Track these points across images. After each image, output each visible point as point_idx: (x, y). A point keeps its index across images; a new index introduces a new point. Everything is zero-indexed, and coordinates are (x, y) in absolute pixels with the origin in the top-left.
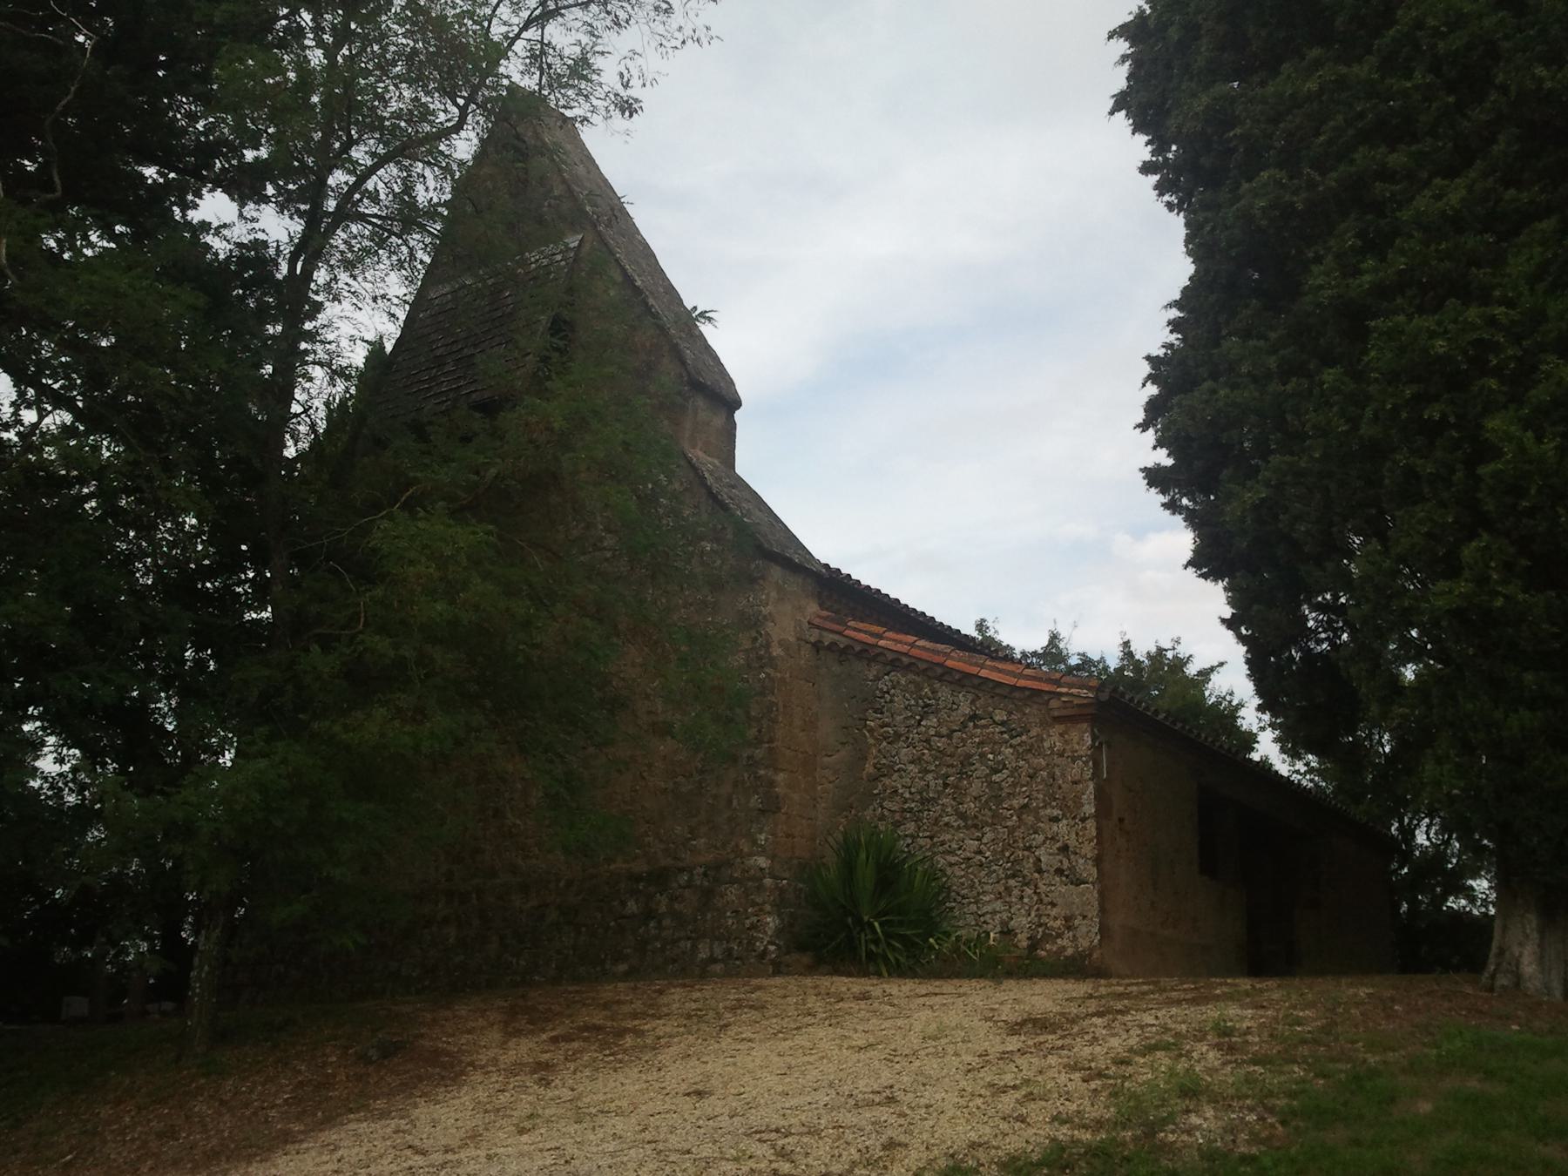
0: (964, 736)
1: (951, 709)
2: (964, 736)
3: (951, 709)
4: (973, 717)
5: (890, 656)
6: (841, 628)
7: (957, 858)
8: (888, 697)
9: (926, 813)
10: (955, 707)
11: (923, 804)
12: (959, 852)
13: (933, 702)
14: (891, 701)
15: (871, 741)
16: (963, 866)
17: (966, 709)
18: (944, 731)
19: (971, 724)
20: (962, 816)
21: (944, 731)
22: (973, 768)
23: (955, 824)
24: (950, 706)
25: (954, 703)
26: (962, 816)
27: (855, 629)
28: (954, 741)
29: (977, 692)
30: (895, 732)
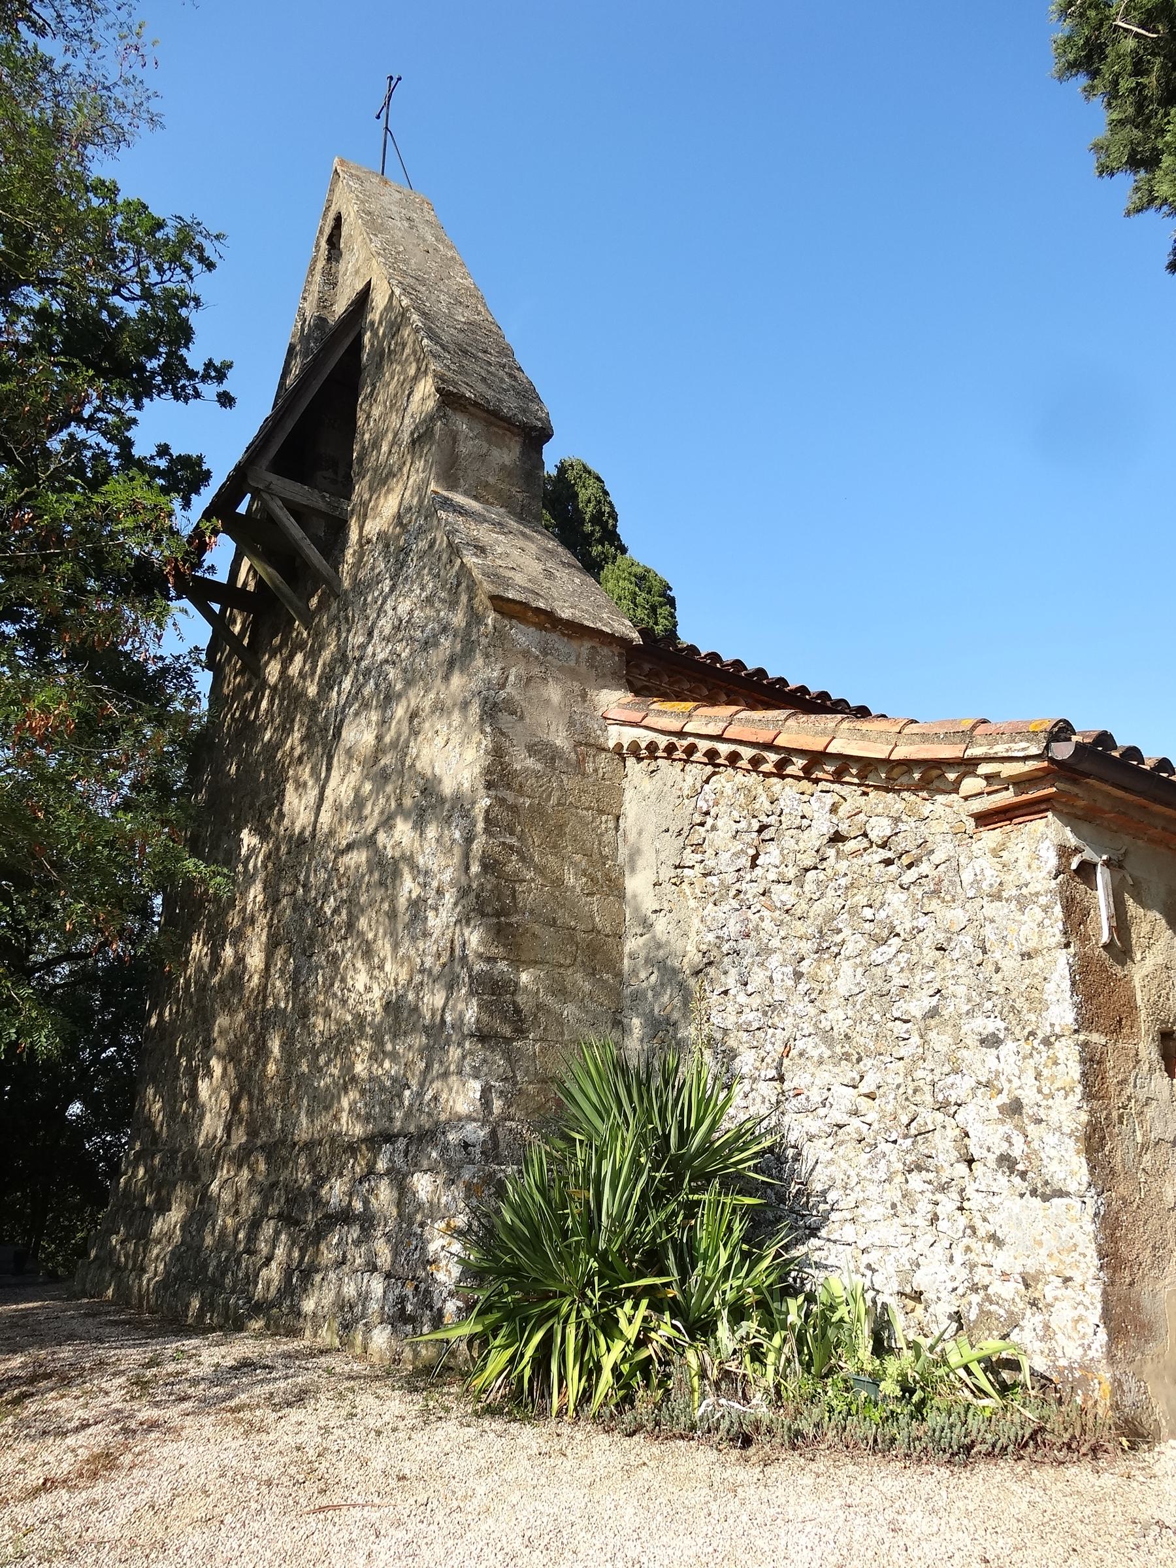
0: (822, 876)
1: (799, 828)
2: (822, 876)
3: (799, 828)
4: (837, 838)
5: (704, 745)
6: (636, 716)
7: (819, 1123)
8: (710, 821)
9: (771, 1031)
10: (805, 822)
11: (765, 1014)
12: (822, 1112)
13: (773, 820)
14: (714, 828)
15: (692, 903)
16: (831, 1141)
17: (823, 826)
18: (791, 873)
19: (831, 853)
20: (827, 1037)
21: (791, 873)
22: (838, 938)
23: (815, 1053)
24: (798, 821)
25: (803, 817)
26: (827, 1037)
27: (661, 713)
28: (807, 888)
29: (836, 787)
30: (722, 882)
